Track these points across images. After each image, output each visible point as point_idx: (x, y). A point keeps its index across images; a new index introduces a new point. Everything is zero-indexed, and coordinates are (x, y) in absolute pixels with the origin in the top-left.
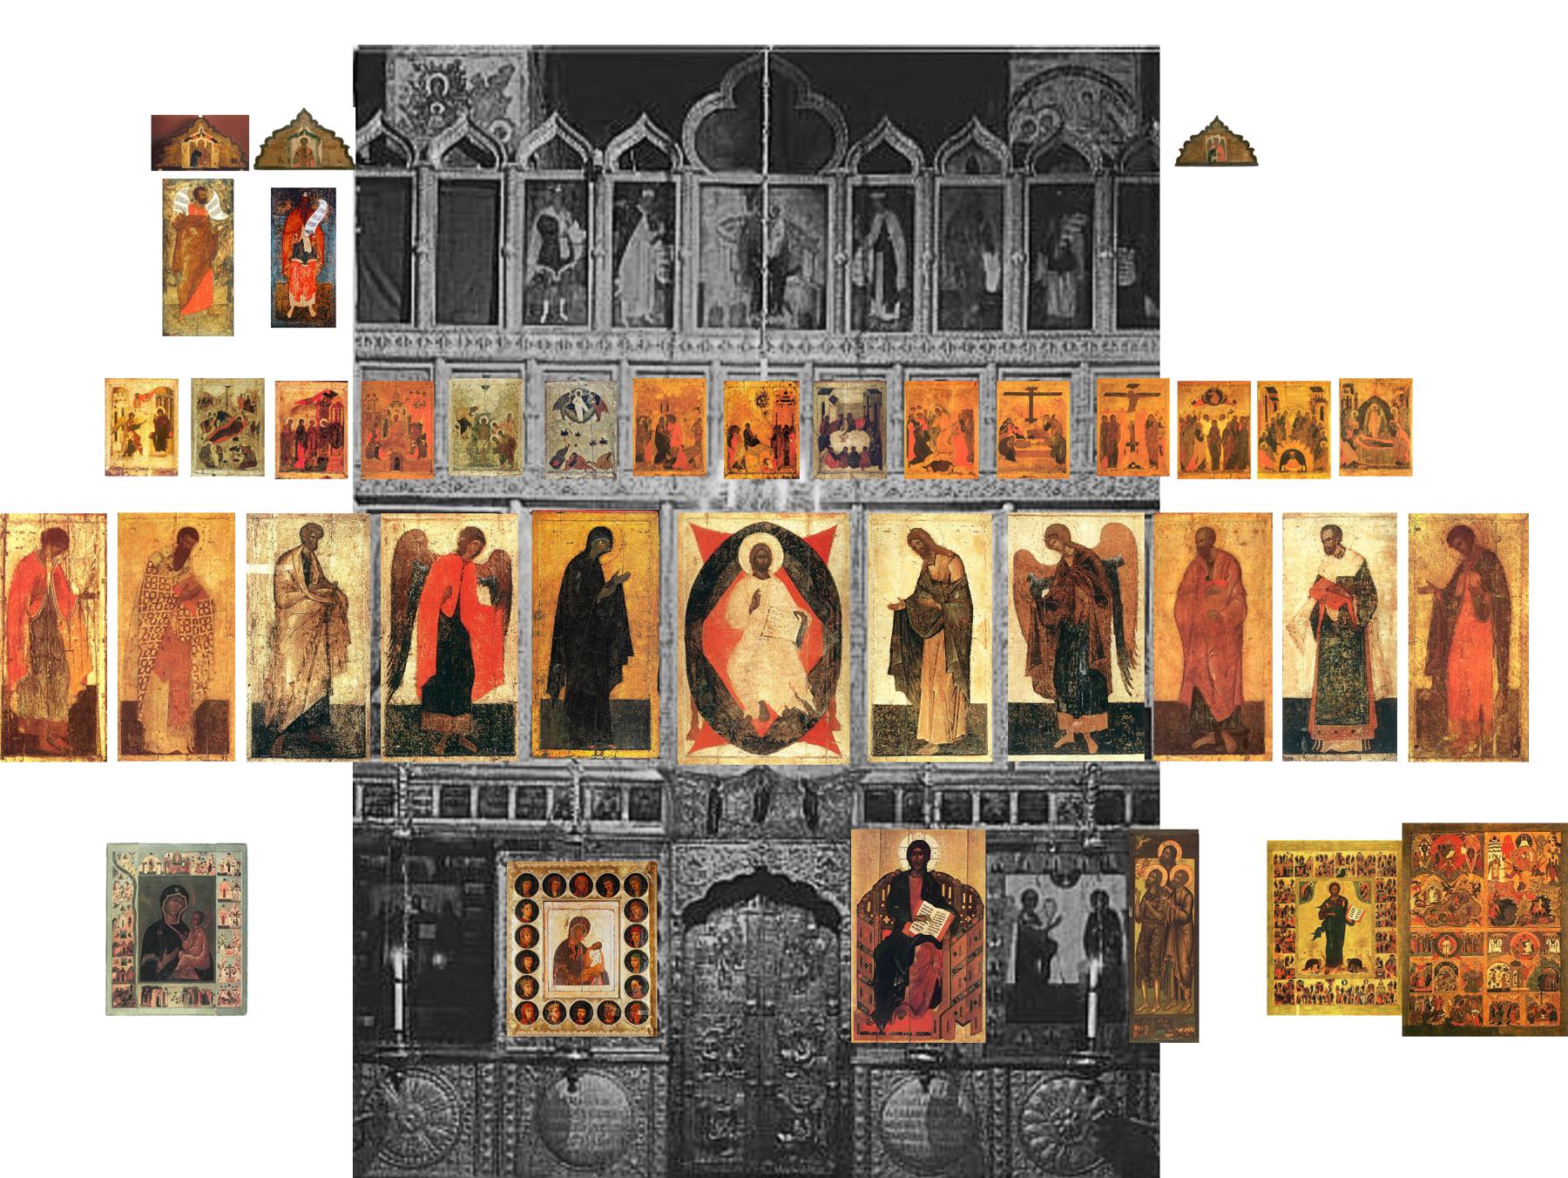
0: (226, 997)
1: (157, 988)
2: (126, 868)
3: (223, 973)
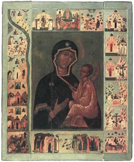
0: (113, 143)
1: (49, 135)
2: (20, 24)
3: (110, 121)
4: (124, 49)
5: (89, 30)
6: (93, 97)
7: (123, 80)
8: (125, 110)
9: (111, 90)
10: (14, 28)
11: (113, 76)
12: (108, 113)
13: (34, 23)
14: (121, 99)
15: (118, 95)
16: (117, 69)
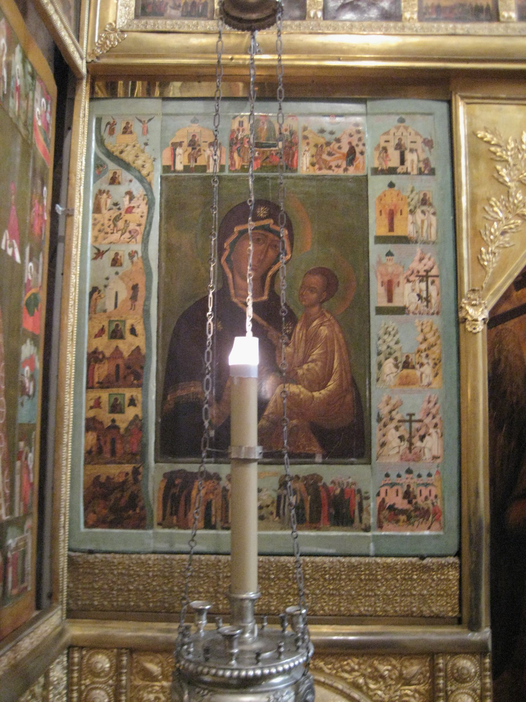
0: (401, 504)
1: (208, 477)
2: (128, 157)
3: (392, 436)
4: (430, 225)
5: (325, 172)
6: (340, 364)
7: (428, 314)
8: (435, 404)
9: (392, 344)
10: (112, 166)
11: (397, 303)
12: (385, 411)
13: (167, 152)
14: (422, 369)
15: (414, 359)
16: (408, 281)
